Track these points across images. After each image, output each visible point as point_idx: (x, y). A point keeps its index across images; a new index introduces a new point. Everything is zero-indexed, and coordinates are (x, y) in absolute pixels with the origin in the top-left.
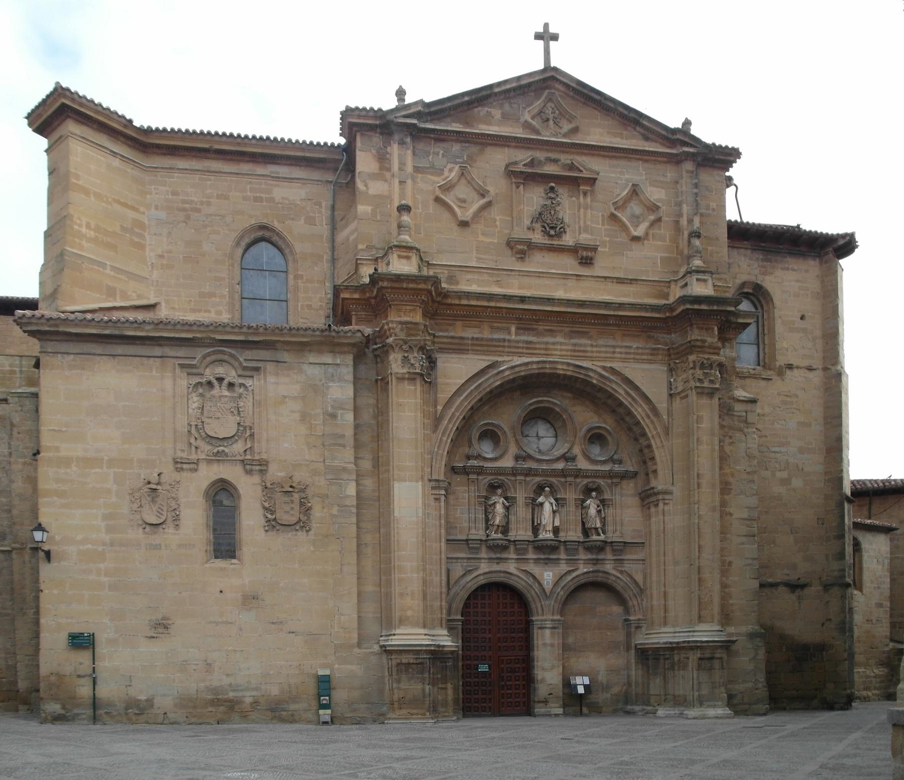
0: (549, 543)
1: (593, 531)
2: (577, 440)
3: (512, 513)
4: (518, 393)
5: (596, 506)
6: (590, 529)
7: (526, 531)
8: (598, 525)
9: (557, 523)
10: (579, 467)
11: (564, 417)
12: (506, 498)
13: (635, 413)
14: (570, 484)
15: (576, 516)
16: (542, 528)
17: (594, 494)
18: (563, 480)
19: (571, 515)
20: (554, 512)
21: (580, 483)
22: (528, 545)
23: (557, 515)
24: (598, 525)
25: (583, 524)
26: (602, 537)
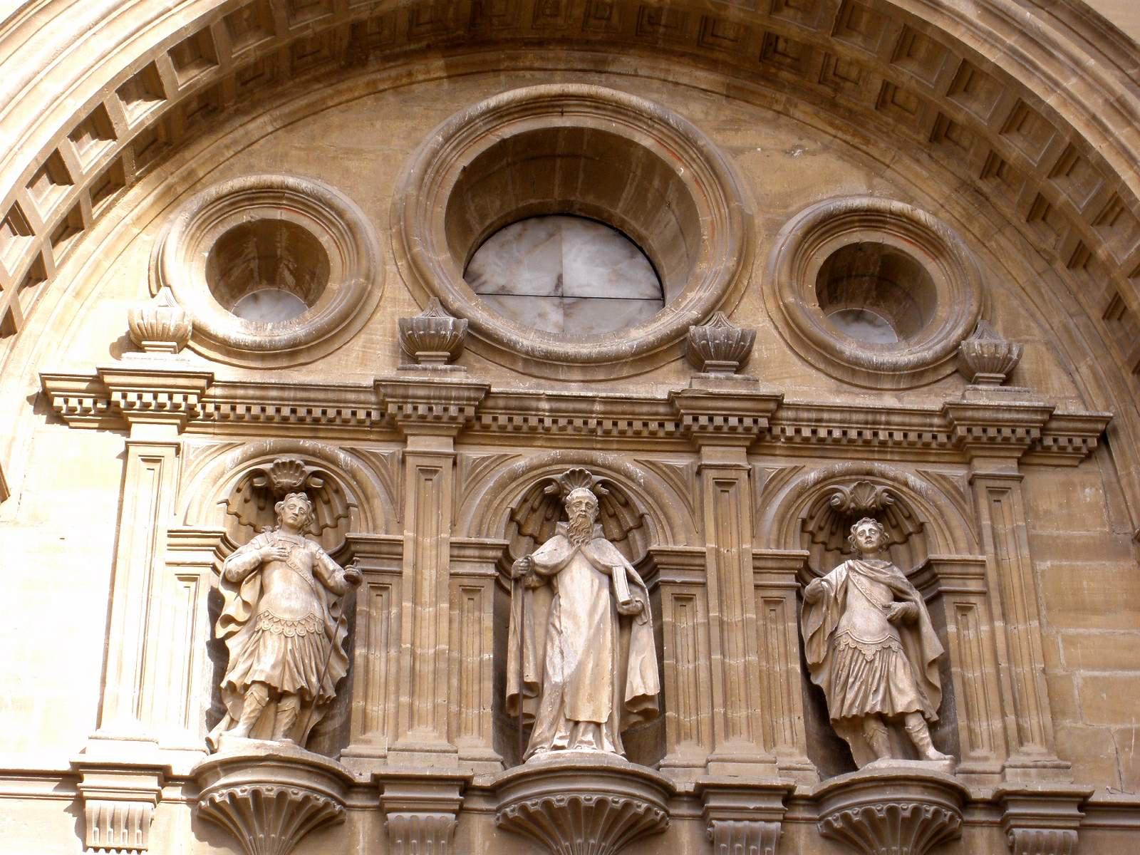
0: (588, 792)
1: (879, 734)
2: (757, 276)
3: (378, 631)
4: (437, 65)
5: (881, 594)
6: (856, 723)
7: (450, 740)
8: (906, 697)
9: (643, 681)
10: (765, 389)
11: (682, 171)
12: (343, 555)
13: (1051, 100)
14: (724, 485)
15: (765, 653)
16: (547, 710)
17: (865, 530)
18: (681, 462)
19: (736, 640)
20: (625, 620)
21: (780, 478)
22: (461, 811)
23: (644, 636)
24: (906, 697)
25: (817, 698)
26: (935, 763)
